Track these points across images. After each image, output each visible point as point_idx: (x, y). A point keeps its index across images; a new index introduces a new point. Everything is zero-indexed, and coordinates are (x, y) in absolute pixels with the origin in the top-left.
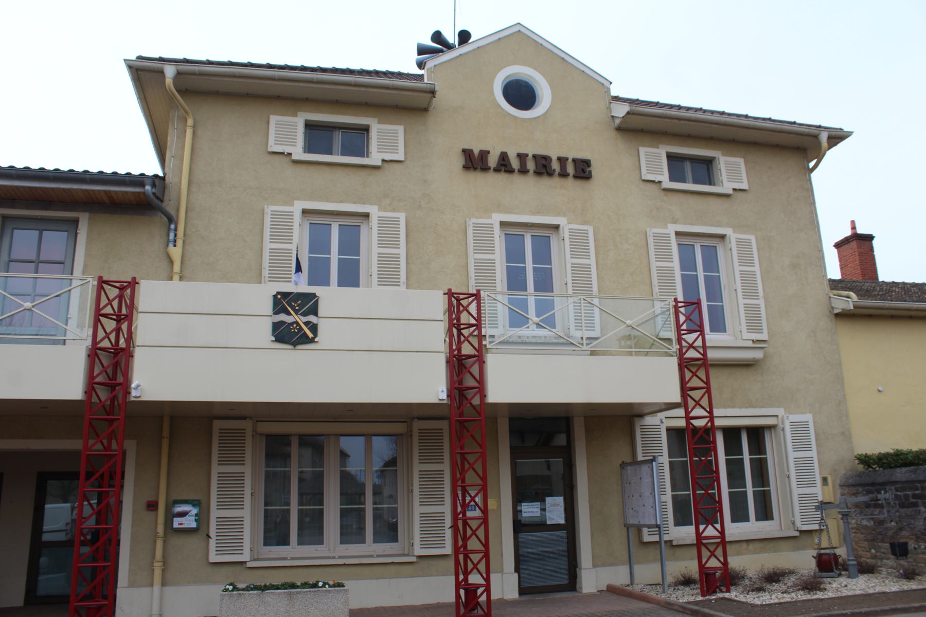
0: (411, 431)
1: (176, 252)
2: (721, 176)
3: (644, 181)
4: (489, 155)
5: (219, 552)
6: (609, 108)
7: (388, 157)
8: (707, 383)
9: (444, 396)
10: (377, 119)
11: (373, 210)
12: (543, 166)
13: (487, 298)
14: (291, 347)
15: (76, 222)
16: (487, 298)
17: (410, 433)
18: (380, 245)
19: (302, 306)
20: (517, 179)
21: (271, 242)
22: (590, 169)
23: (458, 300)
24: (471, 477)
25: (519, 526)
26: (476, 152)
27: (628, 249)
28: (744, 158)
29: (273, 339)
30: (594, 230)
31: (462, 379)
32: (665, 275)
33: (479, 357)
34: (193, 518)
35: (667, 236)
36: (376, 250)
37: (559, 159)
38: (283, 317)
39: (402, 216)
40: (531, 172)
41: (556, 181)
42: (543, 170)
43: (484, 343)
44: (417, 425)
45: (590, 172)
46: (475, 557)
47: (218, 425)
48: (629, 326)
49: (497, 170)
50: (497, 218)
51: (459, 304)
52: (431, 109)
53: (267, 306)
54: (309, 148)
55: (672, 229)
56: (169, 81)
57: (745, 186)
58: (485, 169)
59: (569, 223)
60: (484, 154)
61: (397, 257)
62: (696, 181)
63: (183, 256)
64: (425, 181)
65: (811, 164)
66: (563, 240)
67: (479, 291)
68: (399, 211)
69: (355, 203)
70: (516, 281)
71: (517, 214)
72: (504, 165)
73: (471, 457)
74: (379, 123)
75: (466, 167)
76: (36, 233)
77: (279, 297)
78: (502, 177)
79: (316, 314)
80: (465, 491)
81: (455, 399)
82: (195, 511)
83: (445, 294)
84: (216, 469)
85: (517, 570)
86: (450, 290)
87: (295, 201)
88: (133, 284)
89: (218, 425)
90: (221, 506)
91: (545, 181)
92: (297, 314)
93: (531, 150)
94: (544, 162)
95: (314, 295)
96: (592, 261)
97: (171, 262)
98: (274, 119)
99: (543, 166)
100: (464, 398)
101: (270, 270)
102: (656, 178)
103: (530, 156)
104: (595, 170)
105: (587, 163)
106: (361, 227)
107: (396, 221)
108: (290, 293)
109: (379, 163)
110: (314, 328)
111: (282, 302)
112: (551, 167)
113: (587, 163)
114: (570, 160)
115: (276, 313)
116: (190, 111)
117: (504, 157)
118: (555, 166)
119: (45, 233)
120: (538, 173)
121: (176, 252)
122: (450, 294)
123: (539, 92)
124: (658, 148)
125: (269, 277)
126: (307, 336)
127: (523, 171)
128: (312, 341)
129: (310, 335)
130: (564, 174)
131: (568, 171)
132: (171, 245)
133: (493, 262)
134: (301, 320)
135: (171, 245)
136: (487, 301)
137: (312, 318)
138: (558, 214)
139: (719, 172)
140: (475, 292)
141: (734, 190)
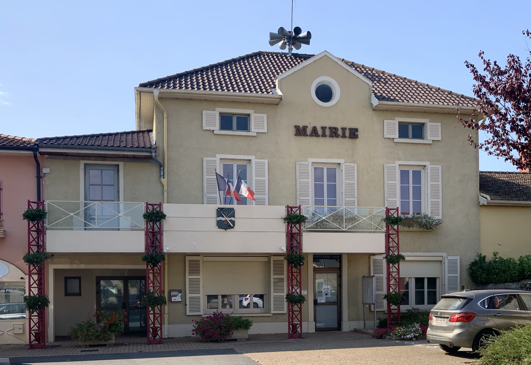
0: (270, 261)
1: (164, 181)
2: (427, 134)
3: (385, 138)
4: (307, 128)
6: (370, 98)
8: (398, 244)
9: (284, 249)
11: (252, 158)
12: (334, 133)
13: (303, 208)
14: (224, 230)
16: (303, 208)
17: (269, 262)
18: (256, 176)
20: (321, 140)
21: (207, 175)
22: (357, 133)
23: (291, 209)
24: (295, 282)
26: (301, 127)
27: (374, 175)
28: (441, 122)
29: (218, 227)
30: (357, 165)
31: (292, 243)
33: (300, 234)
34: (180, 297)
36: (254, 178)
37: (342, 129)
38: (221, 218)
39: (266, 161)
40: (328, 136)
41: (340, 140)
42: (334, 134)
43: (302, 228)
44: (273, 258)
45: (357, 135)
46: (296, 313)
47: (188, 258)
48: (363, 220)
49: (311, 135)
50: (311, 160)
51: (292, 210)
52: (280, 104)
53: (214, 214)
54: (222, 127)
57: (440, 139)
58: (305, 135)
59: (345, 162)
60: (305, 128)
61: (264, 181)
62: (414, 137)
63: (168, 182)
64: (277, 143)
66: (342, 171)
67: (300, 206)
68: (265, 159)
69: (244, 155)
71: (320, 158)
72: (315, 132)
73: (295, 274)
75: (295, 135)
77: (219, 210)
78: (314, 139)
79: (234, 217)
80: (292, 287)
81: (290, 277)
82: (180, 295)
83: (286, 207)
86: (288, 205)
87: (217, 155)
91: (335, 141)
92: (226, 217)
93: (328, 124)
94: (334, 130)
95: (233, 209)
96: (356, 182)
97: (163, 186)
99: (334, 133)
100: (293, 238)
101: (207, 189)
102: (391, 137)
103: (328, 128)
104: (359, 134)
105: (356, 130)
106: (247, 166)
107: (264, 164)
108: (224, 208)
110: (233, 222)
111: (220, 212)
112: (338, 133)
113: (356, 130)
114: (348, 129)
115: (218, 216)
117: (314, 129)
118: (340, 132)
120: (331, 136)
121: (164, 181)
122: (288, 207)
125: (207, 192)
126: (231, 226)
127: (324, 135)
128: (233, 227)
129: (232, 226)
130: (344, 136)
131: (346, 136)
132: (162, 177)
134: (228, 219)
135: (162, 177)
136: (303, 210)
137: (233, 219)
138: (340, 158)
139: (426, 130)
140: (299, 206)
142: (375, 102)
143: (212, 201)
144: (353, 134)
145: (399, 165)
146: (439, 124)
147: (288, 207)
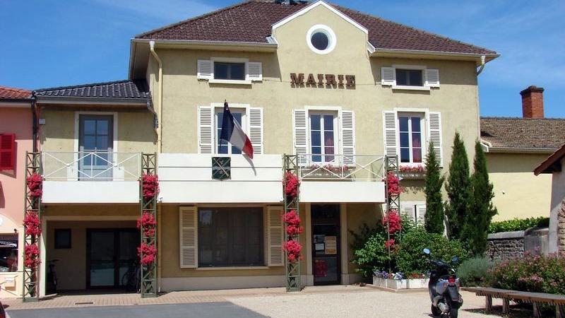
5: (184, 264)
7: (255, 79)
10: (248, 60)
12: (331, 81)
15: (112, 116)
19: (224, 163)
20: (318, 89)
25: (314, 252)
32: (390, 136)
35: (393, 114)
38: (216, 168)
44: (270, 208)
47: (181, 208)
55: (395, 111)
56: (152, 49)
60: (301, 76)
64: (272, 91)
65: (478, 69)
70: (316, 139)
72: (311, 82)
74: (250, 61)
76: (94, 121)
78: (311, 88)
84: (182, 228)
85: (314, 273)
88: (155, 155)
89: (181, 208)
90: (185, 245)
93: (324, 72)
97: (157, 135)
98: (199, 62)
99: (331, 81)
107: (259, 111)
109: (250, 83)
110: (229, 172)
111: (216, 161)
116: (160, 61)
117: (311, 77)
119: (98, 121)
120: (328, 86)
123: (330, 39)
124: (391, 67)
129: (228, 175)
133: (304, 130)
137: (228, 168)
141: (431, 88)
142: (372, 50)
143: (206, 150)
144: (351, 82)
145: (398, 112)
146: (438, 71)
147: (285, 156)
